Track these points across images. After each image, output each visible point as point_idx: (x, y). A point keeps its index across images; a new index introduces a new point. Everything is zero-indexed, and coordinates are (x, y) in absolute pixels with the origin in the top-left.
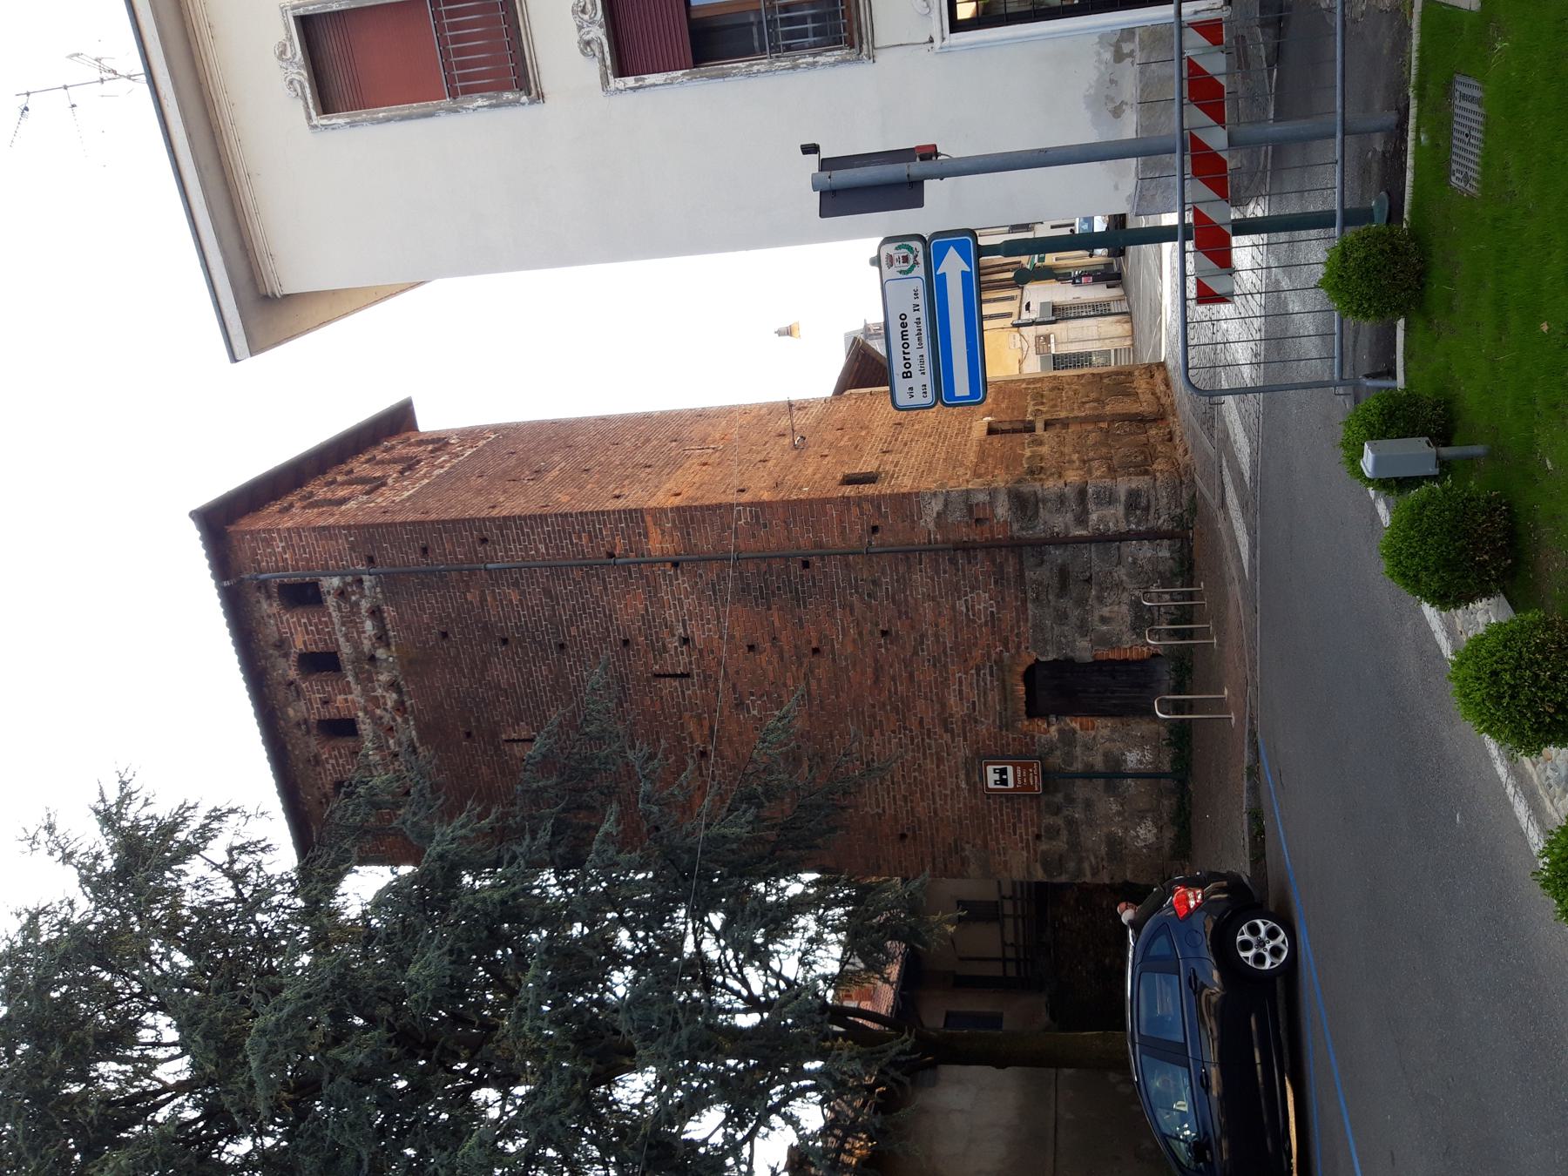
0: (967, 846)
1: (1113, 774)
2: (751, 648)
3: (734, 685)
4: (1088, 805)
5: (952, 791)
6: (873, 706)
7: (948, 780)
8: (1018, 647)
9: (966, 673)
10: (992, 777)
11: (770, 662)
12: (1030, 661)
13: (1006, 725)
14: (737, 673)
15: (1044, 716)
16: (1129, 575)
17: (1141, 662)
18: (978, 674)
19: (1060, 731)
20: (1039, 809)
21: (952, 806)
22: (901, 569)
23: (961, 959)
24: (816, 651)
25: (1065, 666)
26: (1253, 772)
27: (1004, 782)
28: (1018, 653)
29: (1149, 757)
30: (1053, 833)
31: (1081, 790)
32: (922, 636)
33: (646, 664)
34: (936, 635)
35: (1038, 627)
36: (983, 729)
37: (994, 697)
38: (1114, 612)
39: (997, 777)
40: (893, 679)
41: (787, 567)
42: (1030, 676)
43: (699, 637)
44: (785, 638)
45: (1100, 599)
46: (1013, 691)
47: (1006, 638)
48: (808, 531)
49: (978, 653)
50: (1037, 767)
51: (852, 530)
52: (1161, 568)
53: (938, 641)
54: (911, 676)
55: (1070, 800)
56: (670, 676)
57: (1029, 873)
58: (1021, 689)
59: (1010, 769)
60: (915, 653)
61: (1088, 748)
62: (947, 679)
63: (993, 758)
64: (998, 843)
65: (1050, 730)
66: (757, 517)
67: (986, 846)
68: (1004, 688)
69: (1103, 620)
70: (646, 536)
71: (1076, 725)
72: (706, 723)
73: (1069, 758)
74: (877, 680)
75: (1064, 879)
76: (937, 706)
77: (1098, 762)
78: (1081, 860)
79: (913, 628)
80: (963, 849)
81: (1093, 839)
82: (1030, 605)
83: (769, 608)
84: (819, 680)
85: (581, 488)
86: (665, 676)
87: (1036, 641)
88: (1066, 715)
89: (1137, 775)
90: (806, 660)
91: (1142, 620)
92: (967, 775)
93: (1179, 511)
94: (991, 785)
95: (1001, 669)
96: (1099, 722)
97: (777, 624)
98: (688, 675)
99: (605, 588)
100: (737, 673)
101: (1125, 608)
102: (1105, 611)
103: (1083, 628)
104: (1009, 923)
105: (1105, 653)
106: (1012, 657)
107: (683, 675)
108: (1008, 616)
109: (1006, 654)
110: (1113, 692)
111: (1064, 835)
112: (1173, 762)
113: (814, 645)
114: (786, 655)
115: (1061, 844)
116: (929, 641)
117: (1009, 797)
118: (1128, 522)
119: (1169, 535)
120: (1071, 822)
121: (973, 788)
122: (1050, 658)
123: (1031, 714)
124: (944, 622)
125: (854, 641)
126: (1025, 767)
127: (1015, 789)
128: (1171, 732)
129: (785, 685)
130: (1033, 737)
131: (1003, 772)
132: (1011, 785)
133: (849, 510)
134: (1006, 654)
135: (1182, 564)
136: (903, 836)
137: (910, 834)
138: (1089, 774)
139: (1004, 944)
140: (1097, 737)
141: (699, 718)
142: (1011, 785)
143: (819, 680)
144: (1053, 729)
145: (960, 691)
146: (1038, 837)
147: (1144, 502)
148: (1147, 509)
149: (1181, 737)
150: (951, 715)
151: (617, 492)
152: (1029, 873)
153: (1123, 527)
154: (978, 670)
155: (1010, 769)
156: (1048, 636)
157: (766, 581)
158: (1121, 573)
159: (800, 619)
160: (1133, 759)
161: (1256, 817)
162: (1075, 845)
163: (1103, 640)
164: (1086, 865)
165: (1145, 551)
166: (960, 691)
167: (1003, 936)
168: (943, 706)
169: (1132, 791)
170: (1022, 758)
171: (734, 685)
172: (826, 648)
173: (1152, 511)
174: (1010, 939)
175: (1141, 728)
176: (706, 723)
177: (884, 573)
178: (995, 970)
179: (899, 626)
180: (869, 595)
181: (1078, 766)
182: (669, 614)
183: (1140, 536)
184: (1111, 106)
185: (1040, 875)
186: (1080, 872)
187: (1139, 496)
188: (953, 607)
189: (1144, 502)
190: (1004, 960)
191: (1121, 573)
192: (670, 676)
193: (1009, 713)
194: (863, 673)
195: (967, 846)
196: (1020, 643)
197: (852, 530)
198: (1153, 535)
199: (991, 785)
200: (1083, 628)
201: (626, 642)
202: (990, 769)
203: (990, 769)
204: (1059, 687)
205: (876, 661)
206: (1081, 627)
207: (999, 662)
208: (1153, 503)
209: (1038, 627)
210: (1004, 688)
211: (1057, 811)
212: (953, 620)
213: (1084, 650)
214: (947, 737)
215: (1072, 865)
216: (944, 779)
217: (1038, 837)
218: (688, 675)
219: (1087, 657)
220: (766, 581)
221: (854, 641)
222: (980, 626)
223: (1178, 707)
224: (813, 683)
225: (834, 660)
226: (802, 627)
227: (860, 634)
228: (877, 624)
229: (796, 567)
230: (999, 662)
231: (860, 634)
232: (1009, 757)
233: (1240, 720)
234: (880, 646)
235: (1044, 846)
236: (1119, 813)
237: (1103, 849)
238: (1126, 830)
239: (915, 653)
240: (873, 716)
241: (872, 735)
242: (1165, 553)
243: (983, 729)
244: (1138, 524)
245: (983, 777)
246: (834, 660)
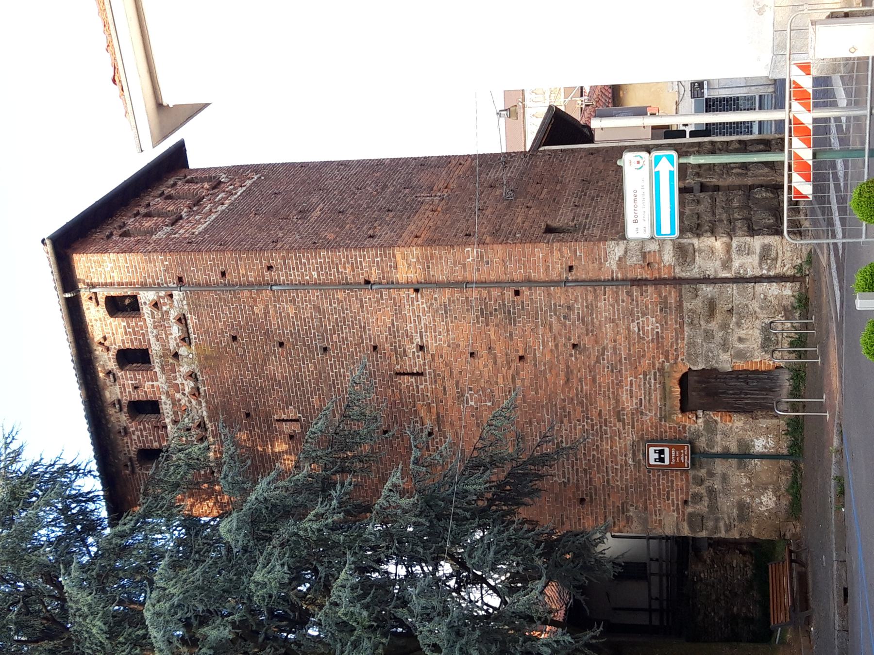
0: (631, 509)
1: (744, 455)
2: (472, 354)
3: (457, 382)
4: (725, 478)
5: (622, 466)
6: (564, 400)
7: (619, 458)
8: (676, 359)
9: (636, 378)
10: (653, 456)
11: (486, 366)
12: (685, 370)
13: (664, 417)
14: (460, 373)
15: (694, 410)
16: (761, 308)
17: (768, 372)
18: (645, 379)
19: (706, 422)
20: (687, 480)
21: (622, 477)
22: (590, 298)
23: (615, 609)
24: (521, 358)
25: (710, 375)
26: (840, 452)
27: (662, 460)
28: (676, 363)
29: (771, 443)
30: (697, 498)
31: (719, 467)
32: (604, 349)
33: (390, 364)
34: (614, 348)
35: (692, 344)
36: (646, 419)
37: (656, 396)
38: (749, 336)
39: (657, 456)
40: (580, 380)
41: (503, 294)
42: (683, 381)
43: (432, 345)
44: (499, 348)
45: (739, 325)
46: (671, 392)
47: (667, 351)
48: (520, 268)
49: (645, 362)
50: (687, 448)
51: (553, 268)
52: (784, 303)
53: (615, 354)
54: (594, 380)
55: (711, 474)
56: (408, 374)
57: (678, 529)
58: (677, 390)
59: (667, 450)
60: (598, 361)
61: (725, 435)
62: (621, 381)
63: (653, 441)
64: (655, 506)
65: (696, 423)
66: (482, 257)
67: (646, 508)
68: (664, 388)
69: (740, 340)
70: (396, 268)
71: (718, 419)
72: (434, 410)
73: (711, 443)
74: (568, 381)
75: (704, 534)
76: (612, 402)
77: (734, 448)
78: (717, 520)
79: (596, 342)
80: (628, 511)
81: (727, 505)
82: (686, 328)
83: (487, 325)
84: (523, 380)
85: (342, 228)
86: (404, 374)
87: (689, 354)
88: (710, 409)
89: (762, 456)
90: (513, 365)
91: (768, 343)
92: (634, 454)
93: (799, 261)
94: (652, 462)
95: (662, 375)
96: (735, 417)
97: (493, 337)
98: (422, 374)
99: (362, 307)
100: (460, 373)
101: (757, 333)
102: (742, 333)
103: (725, 346)
104: (655, 580)
105: (741, 365)
106: (672, 366)
107: (418, 374)
108: (670, 335)
109: (667, 364)
110: (746, 394)
111: (706, 502)
112: (790, 447)
113: (520, 354)
114: (499, 361)
115: (703, 507)
116: (609, 353)
117: (664, 470)
118: (762, 268)
119: (791, 279)
120: (711, 491)
121: (637, 463)
122: (700, 368)
123: (683, 410)
124: (621, 338)
125: (551, 351)
126: (679, 449)
127: (670, 465)
128: (788, 424)
129: (497, 383)
130: (684, 427)
131: (662, 452)
132: (667, 462)
133: (552, 253)
134: (667, 364)
135: (800, 301)
136: (582, 501)
137: (588, 499)
138: (726, 455)
139: (651, 598)
140: (732, 429)
141: (429, 406)
142: (667, 462)
143: (523, 380)
144: (700, 421)
145: (631, 391)
146: (686, 502)
147: (773, 255)
148: (776, 259)
149: (796, 427)
150: (623, 409)
151: (371, 232)
152: (678, 529)
153: (758, 272)
154: (645, 375)
155: (667, 450)
156: (699, 351)
157: (486, 304)
158: (755, 305)
159: (511, 334)
160: (760, 445)
161: (840, 480)
162: (713, 507)
163: (740, 355)
164: (721, 524)
165: (773, 290)
166: (631, 391)
167: (650, 590)
168: (617, 401)
169: (758, 468)
170: (676, 441)
171: (457, 382)
172: (530, 357)
173: (779, 261)
174: (655, 592)
175: (764, 423)
176: (434, 410)
177: (576, 301)
178: (642, 619)
179: (587, 341)
180: (565, 317)
181: (717, 449)
182: (410, 326)
183: (770, 279)
184: (757, 7)
185: (686, 531)
186: (716, 528)
187: (770, 250)
188: (628, 328)
189: (773, 255)
190: (650, 611)
191: (755, 305)
192: (408, 374)
193: (667, 408)
194: (557, 375)
195: (631, 509)
196: (677, 356)
197: (553, 268)
198: (781, 279)
199: (652, 462)
200: (725, 346)
201: (375, 348)
202: (652, 449)
203: (652, 449)
204: (704, 390)
205: (568, 367)
206: (724, 345)
207: (661, 369)
208: (780, 255)
209: (692, 344)
210: (664, 388)
211: (701, 482)
212: (628, 338)
213: (725, 362)
214: (619, 425)
215: (710, 524)
216: (616, 457)
217: (686, 502)
218: (422, 374)
219: (728, 368)
220: (486, 304)
221: (551, 351)
222: (648, 342)
223: (794, 407)
224: (519, 383)
225: (535, 365)
226: (512, 339)
227: (556, 346)
228: (570, 339)
229: (509, 294)
230: (661, 369)
231: (556, 346)
232: (666, 441)
233: (833, 416)
234: (571, 355)
235: (690, 510)
236: (748, 485)
237: (735, 512)
238: (752, 497)
239: (598, 361)
240: (563, 408)
241: (562, 422)
242: (789, 293)
243: (646, 419)
244: (769, 270)
245: (646, 455)
246: (535, 365)
